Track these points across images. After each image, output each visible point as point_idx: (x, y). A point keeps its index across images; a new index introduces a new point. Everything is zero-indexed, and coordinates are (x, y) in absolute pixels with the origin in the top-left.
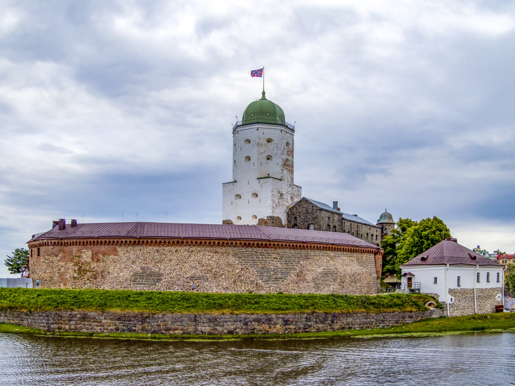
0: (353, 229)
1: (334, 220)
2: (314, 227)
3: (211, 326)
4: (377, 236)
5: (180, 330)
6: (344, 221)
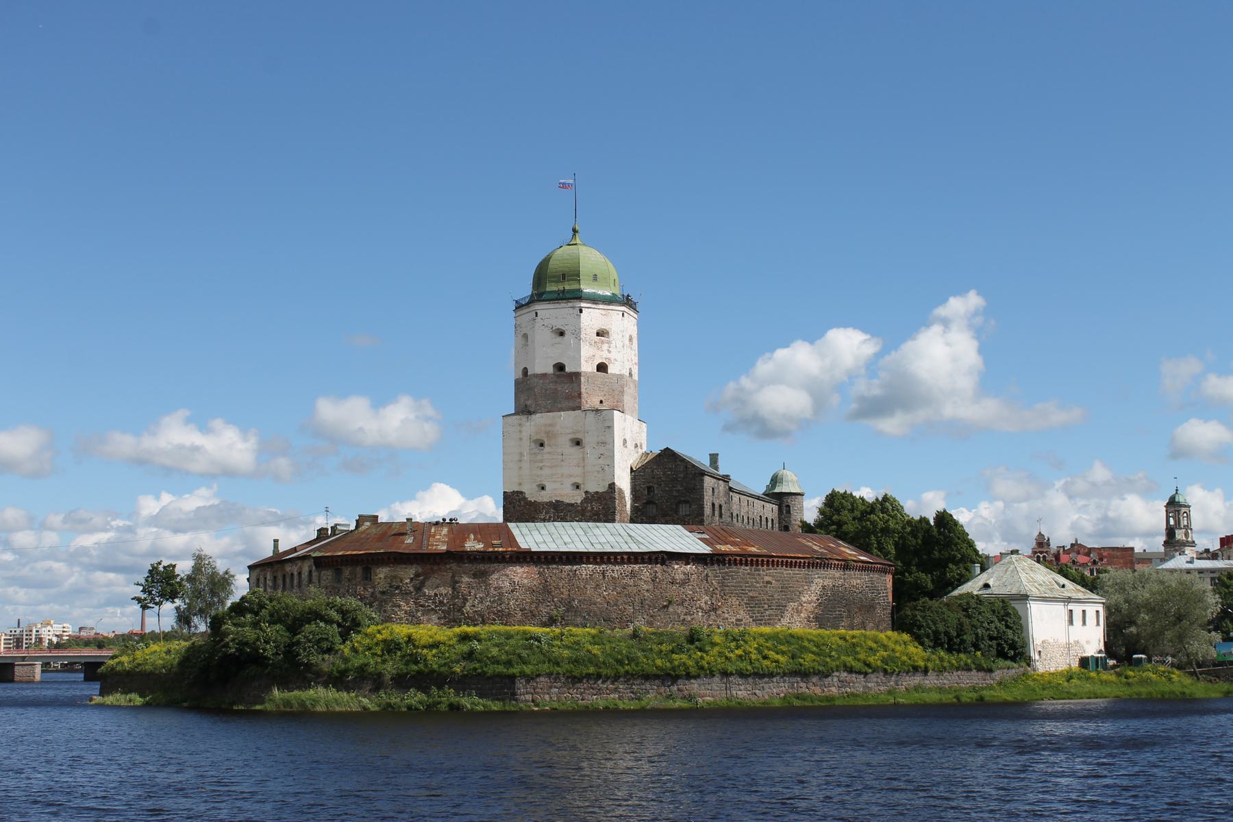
0: (742, 510)
1: (719, 492)
2: (690, 507)
3: (749, 688)
4: (772, 520)
5: (709, 696)
6: (731, 493)
